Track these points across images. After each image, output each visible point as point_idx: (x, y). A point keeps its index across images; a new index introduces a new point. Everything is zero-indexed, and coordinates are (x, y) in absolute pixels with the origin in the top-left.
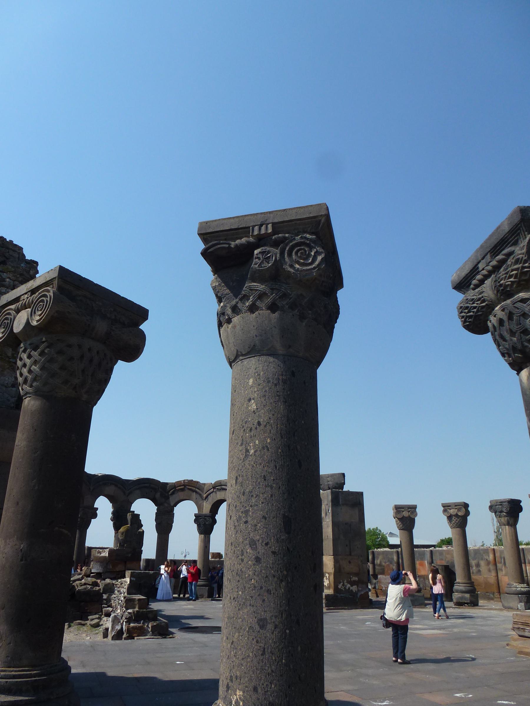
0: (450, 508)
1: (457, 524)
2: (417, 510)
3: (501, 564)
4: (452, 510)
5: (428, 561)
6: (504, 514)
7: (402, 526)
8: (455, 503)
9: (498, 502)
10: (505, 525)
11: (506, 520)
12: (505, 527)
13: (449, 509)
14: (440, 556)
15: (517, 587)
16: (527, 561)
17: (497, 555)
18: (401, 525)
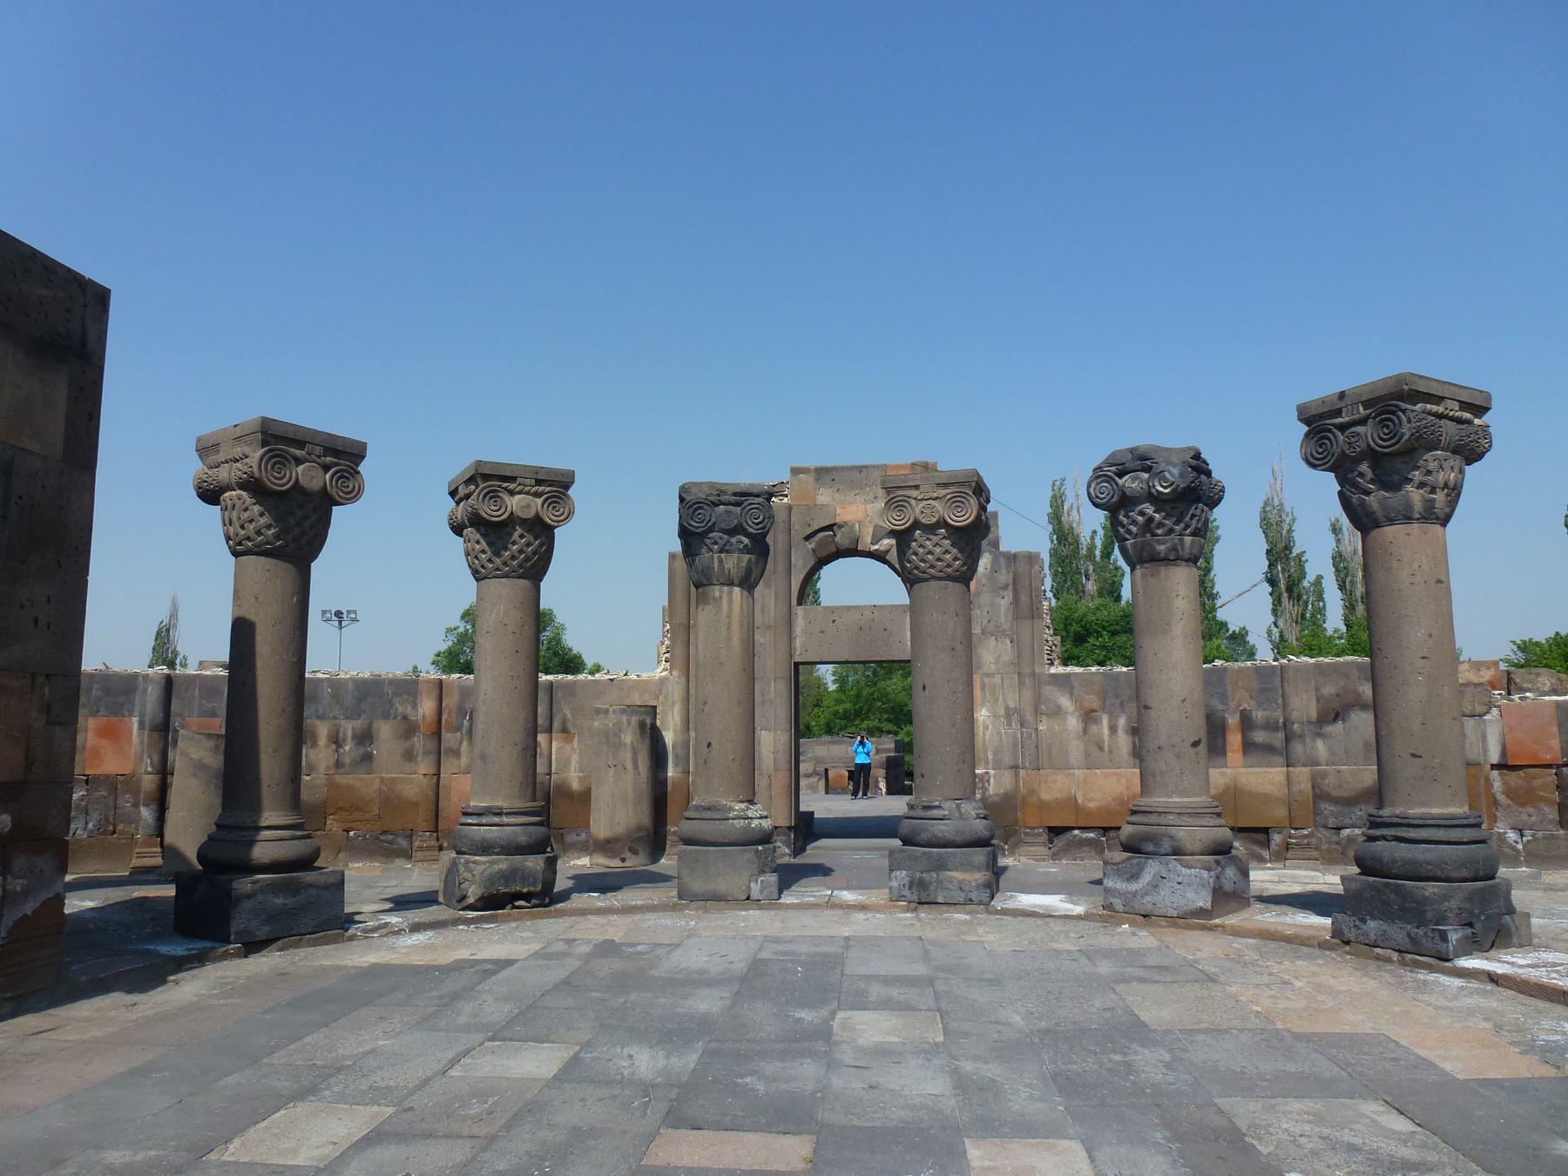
0: (512, 486)
1: (527, 560)
2: (363, 468)
3: (459, 734)
4: (518, 497)
5: (147, 719)
6: (746, 541)
7: (277, 537)
8: (536, 470)
9: (729, 493)
10: (731, 584)
11: (744, 564)
12: (730, 593)
13: (505, 489)
14: (204, 702)
15: (748, 818)
16: (556, 725)
17: (451, 701)
18: (269, 527)
